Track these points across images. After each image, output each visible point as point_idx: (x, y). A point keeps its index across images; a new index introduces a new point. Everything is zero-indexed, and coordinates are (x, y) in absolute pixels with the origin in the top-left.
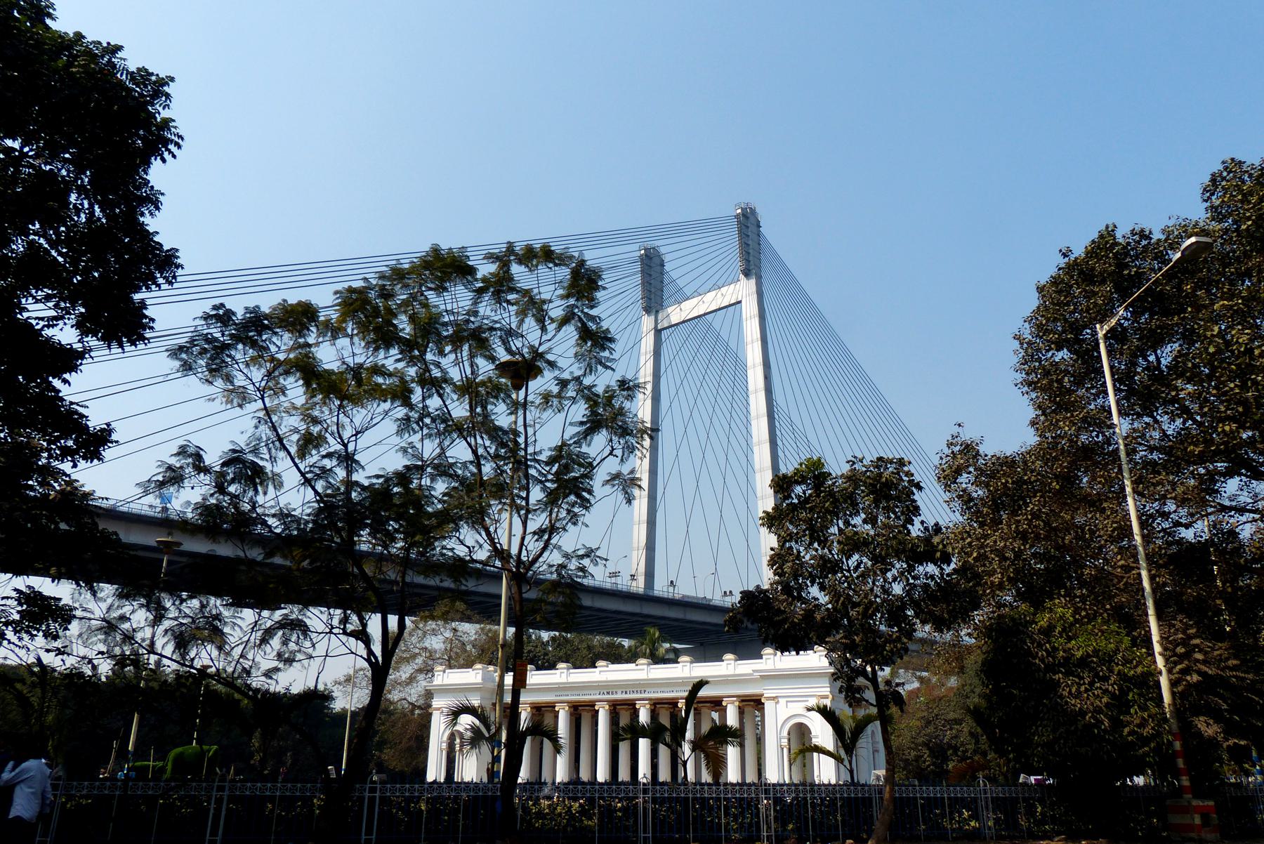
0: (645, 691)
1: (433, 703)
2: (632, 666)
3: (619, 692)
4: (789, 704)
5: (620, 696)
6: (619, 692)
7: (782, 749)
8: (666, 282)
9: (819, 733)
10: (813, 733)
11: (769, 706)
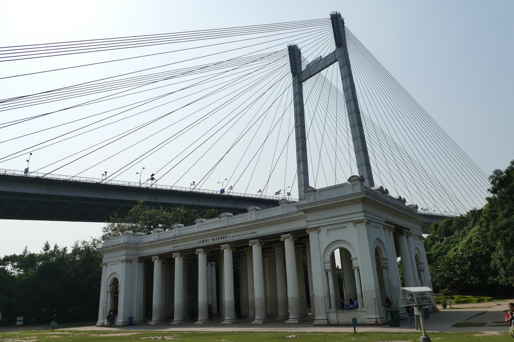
0: (226, 237)
1: (103, 261)
2: (217, 219)
3: (210, 239)
4: (330, 232)
5: (210, 242)
6: (210, 240)
7: (327, 273)
8: (302, 60)
9: (358, 256)
10: (353, 256)
11: (313, 237)
